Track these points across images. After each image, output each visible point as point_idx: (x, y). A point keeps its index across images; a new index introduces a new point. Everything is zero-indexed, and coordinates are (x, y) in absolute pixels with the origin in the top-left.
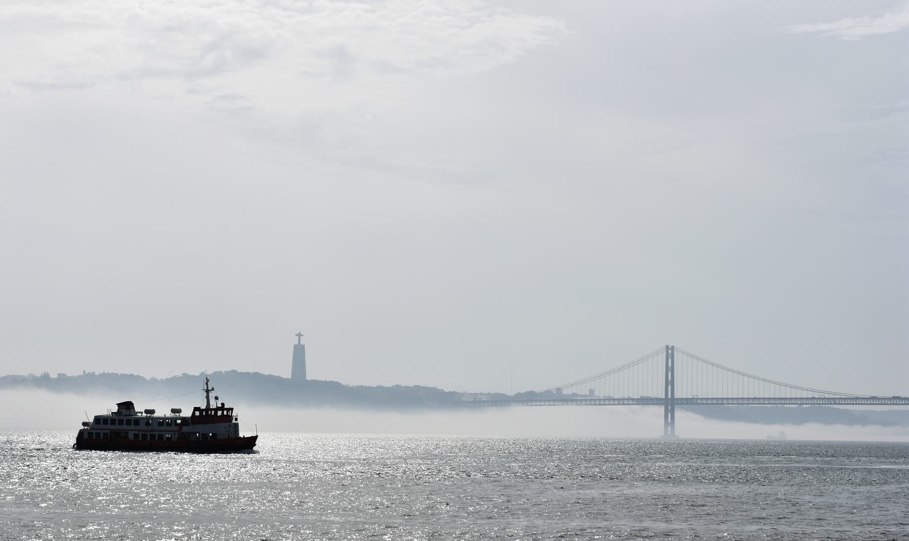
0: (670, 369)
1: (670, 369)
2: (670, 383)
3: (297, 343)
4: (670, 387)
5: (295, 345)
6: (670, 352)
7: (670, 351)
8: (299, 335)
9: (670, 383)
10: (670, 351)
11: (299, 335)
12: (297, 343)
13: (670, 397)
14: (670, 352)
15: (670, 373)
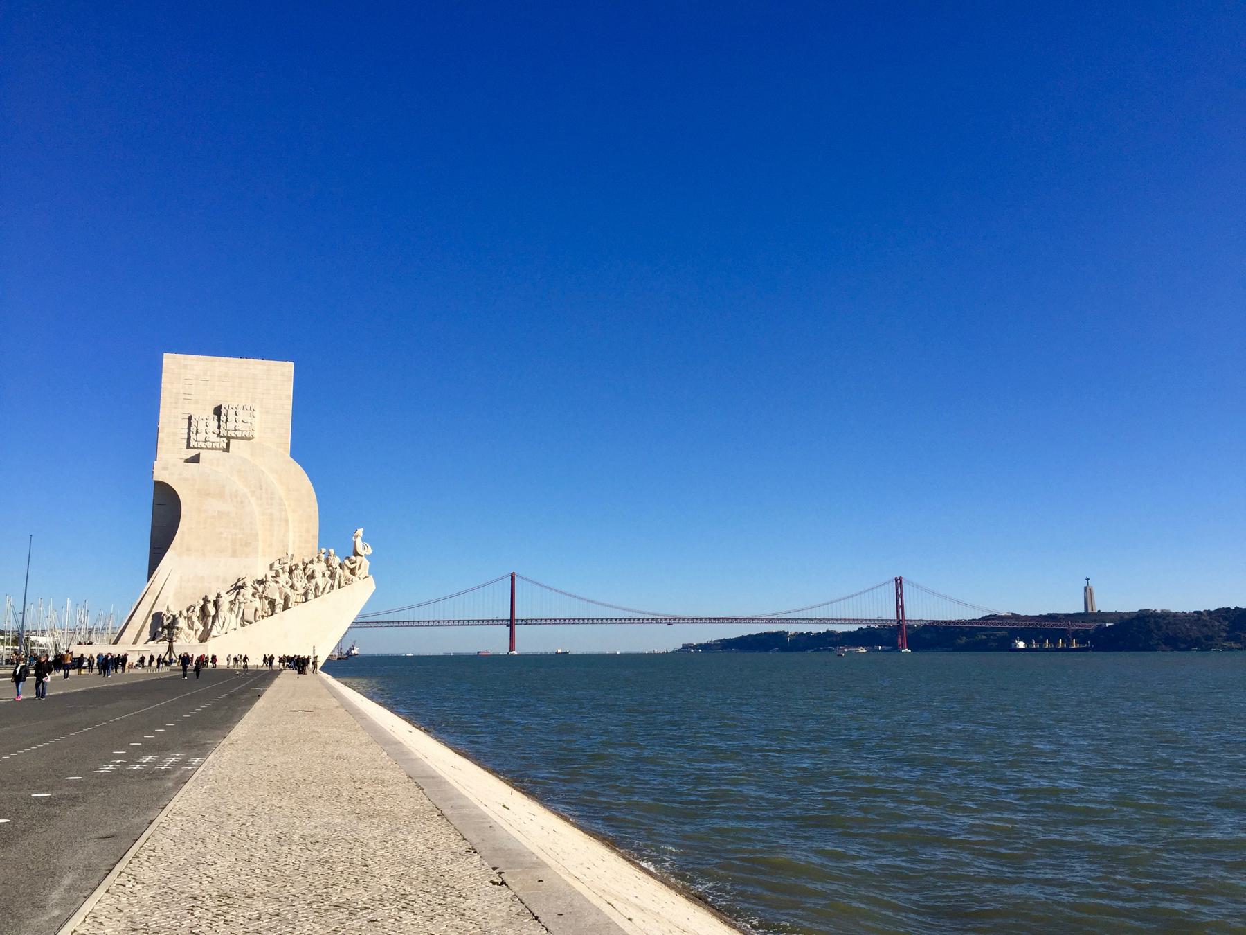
0: (899, 596)
1: (899, 596)
2: (900, 607)
3: (1086, 585)
4: (900, 610)
5: (1086, 588)
6: (899, 582)
7: (899, 581)
8: (1088, 579)
9: (900, 607)
10: (899, 581)
11: (1088, 579)
12: (1086, 585)
13: (901, 618)
14: (899, 582)
15: (900, 600)
